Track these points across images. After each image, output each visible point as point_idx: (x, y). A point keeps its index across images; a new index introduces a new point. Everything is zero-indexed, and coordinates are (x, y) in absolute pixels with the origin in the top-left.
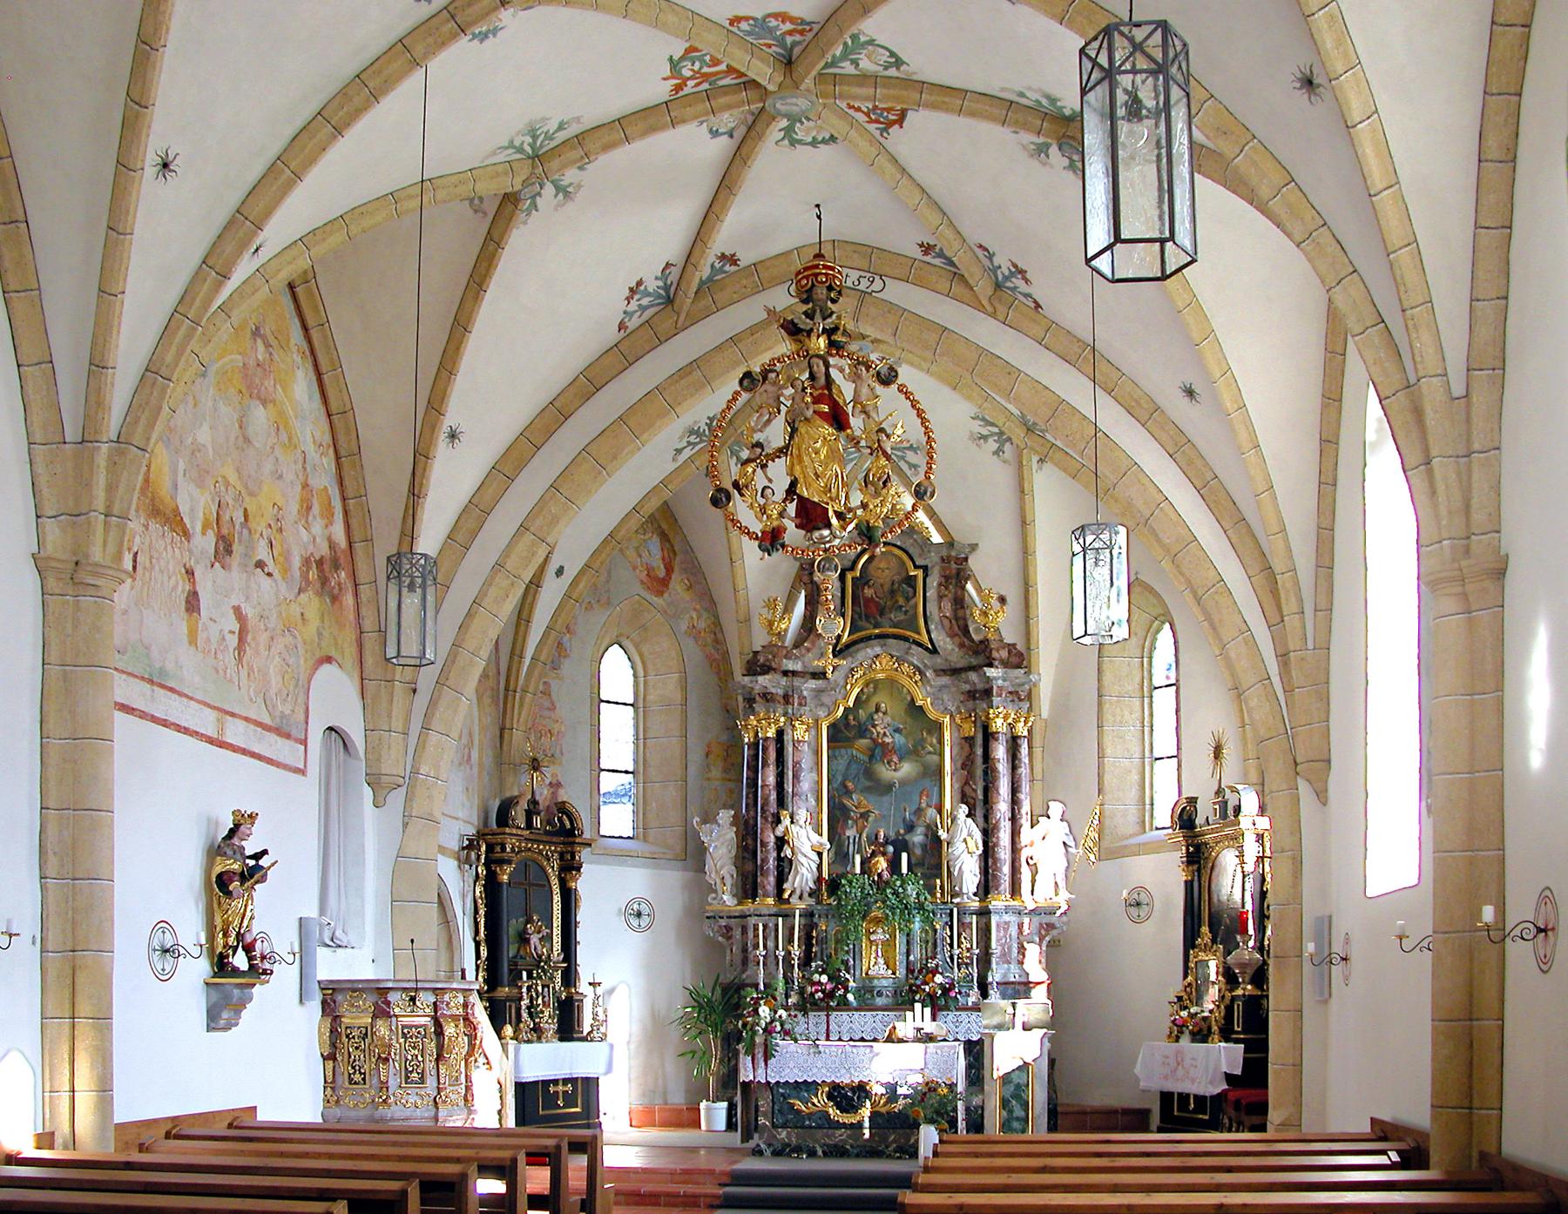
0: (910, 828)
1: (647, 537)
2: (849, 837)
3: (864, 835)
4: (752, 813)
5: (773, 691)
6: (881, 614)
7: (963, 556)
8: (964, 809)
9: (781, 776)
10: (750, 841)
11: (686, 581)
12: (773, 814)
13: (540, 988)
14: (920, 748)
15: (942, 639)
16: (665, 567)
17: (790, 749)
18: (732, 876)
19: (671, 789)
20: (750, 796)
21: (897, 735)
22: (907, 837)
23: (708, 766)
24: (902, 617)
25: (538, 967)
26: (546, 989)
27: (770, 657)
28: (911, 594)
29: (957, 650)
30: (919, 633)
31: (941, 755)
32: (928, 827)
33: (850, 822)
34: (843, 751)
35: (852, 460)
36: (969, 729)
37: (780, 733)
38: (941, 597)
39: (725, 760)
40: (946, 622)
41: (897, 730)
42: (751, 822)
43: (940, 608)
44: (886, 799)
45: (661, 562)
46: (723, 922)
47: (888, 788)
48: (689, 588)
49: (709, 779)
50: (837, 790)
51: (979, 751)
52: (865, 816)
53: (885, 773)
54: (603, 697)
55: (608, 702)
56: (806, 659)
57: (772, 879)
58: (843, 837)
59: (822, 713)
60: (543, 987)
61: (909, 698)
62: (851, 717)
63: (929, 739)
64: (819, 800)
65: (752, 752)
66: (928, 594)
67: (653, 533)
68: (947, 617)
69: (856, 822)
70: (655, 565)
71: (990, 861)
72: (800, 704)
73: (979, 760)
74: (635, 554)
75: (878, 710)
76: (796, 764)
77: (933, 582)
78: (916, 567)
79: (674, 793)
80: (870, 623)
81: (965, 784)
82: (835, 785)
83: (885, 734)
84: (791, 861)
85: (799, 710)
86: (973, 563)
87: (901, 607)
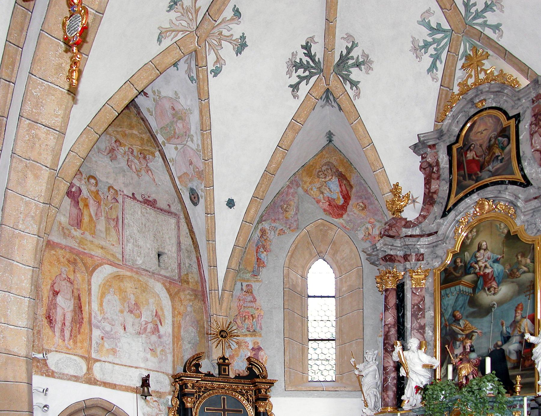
14: (515, 270)
21: (496, 265)
22: (504, 347)
33: (458, 343)
34: (453, 289)
41: (496, 261)
44: (487, 319)
47: (487, 310)
61: (506, 231)
62: (458, 261)
75: (479, 249)
82: (447, 317)
83: (486, 267)
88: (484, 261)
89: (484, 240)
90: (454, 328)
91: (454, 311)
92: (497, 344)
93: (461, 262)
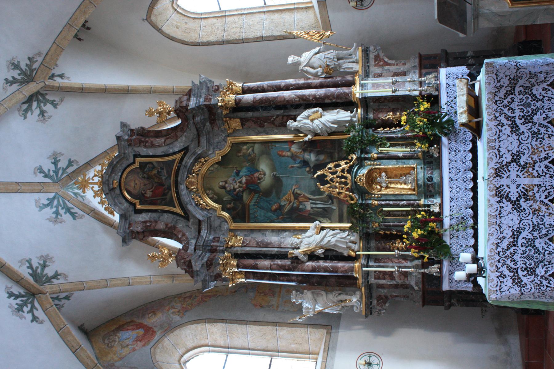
0: (305, 163)
1: (117, 340)
2: (312, 208)
3: (312, 197)
4: (294, 278)
5: (205, 259)
6: (162, 185)
7: (129, 132)
8: (291, 124)
9: (266, 256)
10: (314, 280)
11: (150, 315)
12: (292, 263)
14: (250, 158)
15: (178, 145)
16: (138, 329)
17: (248, 249)
18: (340, 294)
19: (282, 334)
20: (281, 278)
21: (241, 174)
22: (312, 165)
23: (269, 307)
24: (165, 171)
27: (182, 261)
28: (150, 166)
29: (185, 134)
30: (175, 160)
31: (254, 142)
32: (304, 150)
33: (301, 207)
34: (251, 212)
35: (64, 203)
36: (235, 123)
37: (237, 256)
38: (153, 146)
39: (266, 294)
40: (168, 141)
41: (238, 173)
42: (300, 278)
43: (159, 146)
44: (284, 180)
45: (134, 331)
46: (375, 302)
47: (277, 181)
48: (154, 313)
49: (278, 307)
50: (278, 216)
51: (250, 114)
52: (296, 196)
53: (266, 182)
56: (189, 237)
57: (340, 264)
58: (311, 212)
59: (225, 226)
61: (216, 166)
62: (229, 206)
63: (244, 151)
64: (284, 230)
65: (251, 276)
66: (151, 154)
67: (116, 336)
68: (165, 141)
69: (301, 203)
70: (135, 336)
71: (327, 101)
72: (218, 241)
73: (256, 114)
74: (126, 349)
75: (224, 187)
76: (258, 245)
77: (144, 151)
78: (134, 162)
79: (285, 332)
80: (168, 192)
81: (274, 124)
82: (275, 217)
83: (240, 182)
84: (327, 250)
85: (221, 242)
86: (134, 125)
87: (158, 171)
88: (235, 184)
89: (217, 183)
90: (286, 210)
91: (271, 211)
92: (308, 172)
93: (230, 204)
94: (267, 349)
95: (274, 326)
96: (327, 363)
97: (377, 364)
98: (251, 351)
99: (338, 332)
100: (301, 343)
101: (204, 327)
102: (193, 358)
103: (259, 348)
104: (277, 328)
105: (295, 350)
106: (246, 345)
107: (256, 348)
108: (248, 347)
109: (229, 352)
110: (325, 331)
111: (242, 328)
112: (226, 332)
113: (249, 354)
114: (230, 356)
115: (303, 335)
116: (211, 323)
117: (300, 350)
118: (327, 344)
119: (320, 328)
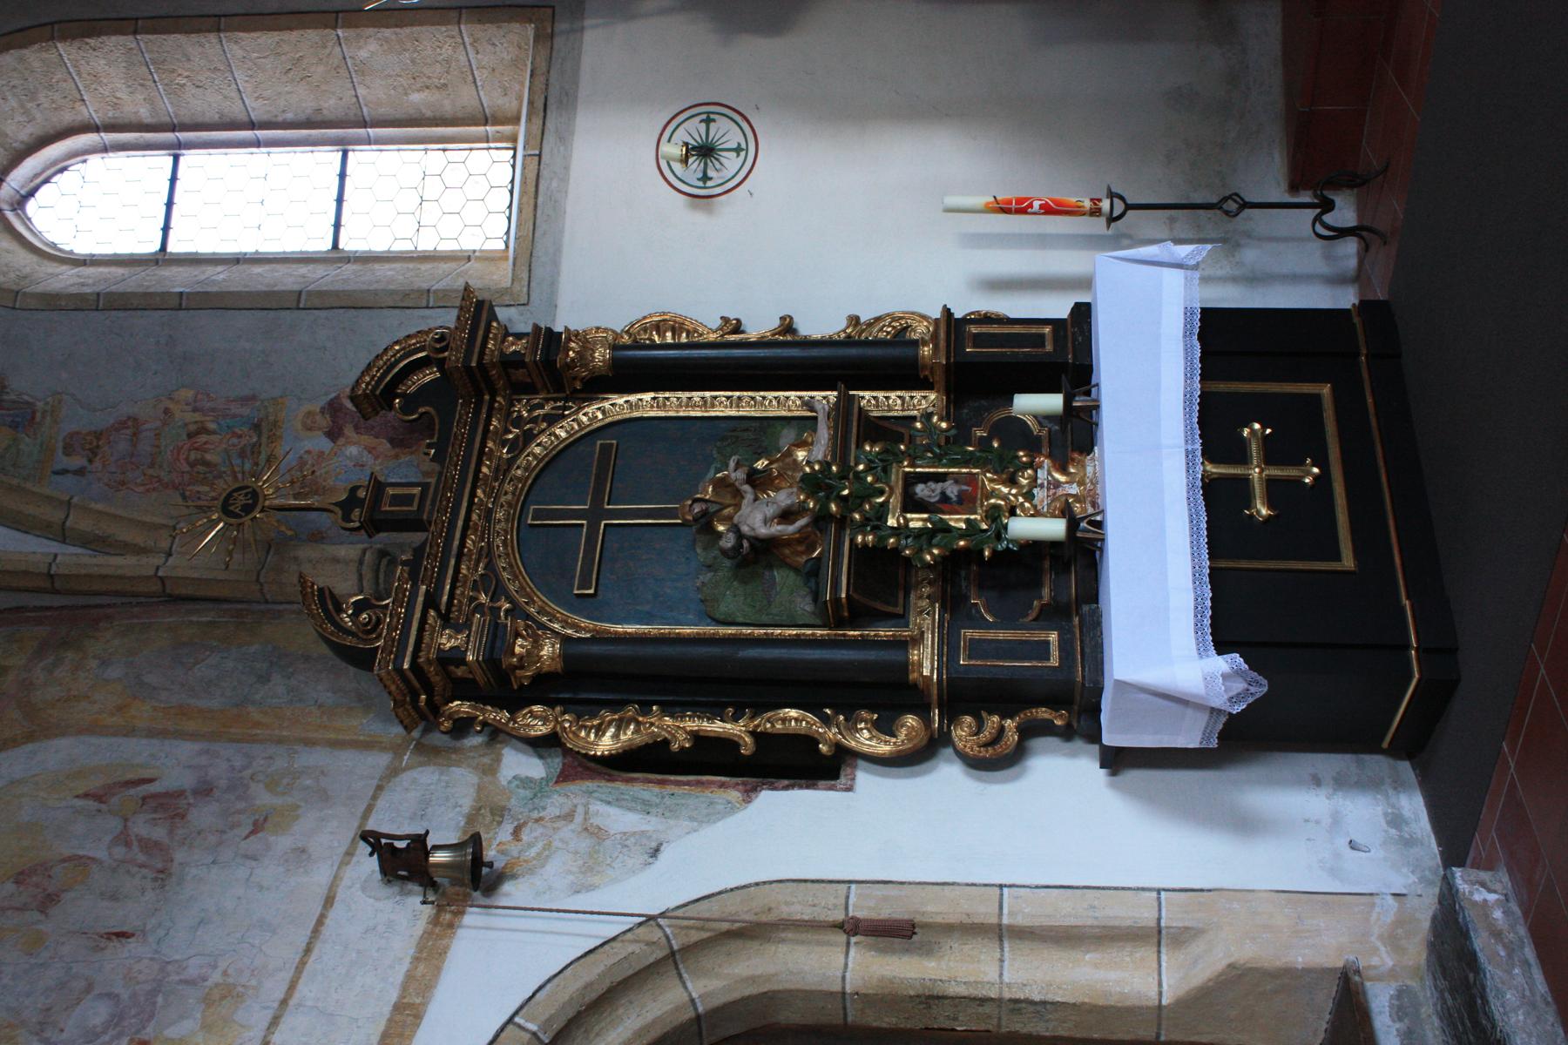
13: (917, 521)
19: (363, 54)
25: (843, 522)
26: (921, 490)
54: (156, 247)
55: (166, 229)
60: (911, 504)
79: (373, 46)
94: (319, 118)
95: (326, 27)
96: (544, 157)
97: (738, 150)
98: (262, 134)
99: (582, 29)
100: (445, 85)
101: (51, 56)
102: (47, 181)
103: (290, 116)
104: (340, 32)
105: (429, 114)
106: (236, 111)
107: (280, 119)
108: (246, 119)
109: (180, 145)
110: (530, 30)
111: (202, 46)
112: (144, 69)
113: (257, 144)
114: (189, 159)
115: (447, 51)
116: (74, 38)
117: (447, 107)
118: (540, 80)
119: (510, 20)
